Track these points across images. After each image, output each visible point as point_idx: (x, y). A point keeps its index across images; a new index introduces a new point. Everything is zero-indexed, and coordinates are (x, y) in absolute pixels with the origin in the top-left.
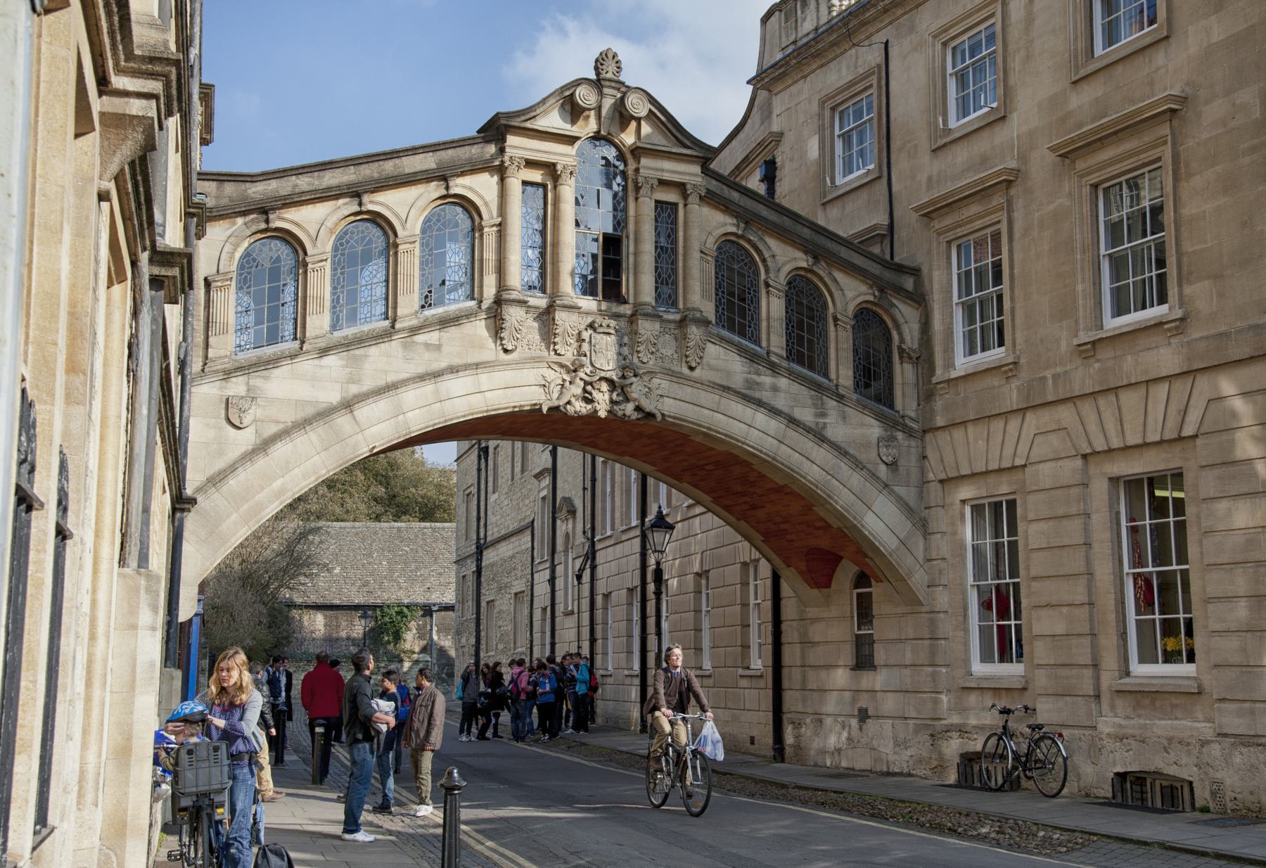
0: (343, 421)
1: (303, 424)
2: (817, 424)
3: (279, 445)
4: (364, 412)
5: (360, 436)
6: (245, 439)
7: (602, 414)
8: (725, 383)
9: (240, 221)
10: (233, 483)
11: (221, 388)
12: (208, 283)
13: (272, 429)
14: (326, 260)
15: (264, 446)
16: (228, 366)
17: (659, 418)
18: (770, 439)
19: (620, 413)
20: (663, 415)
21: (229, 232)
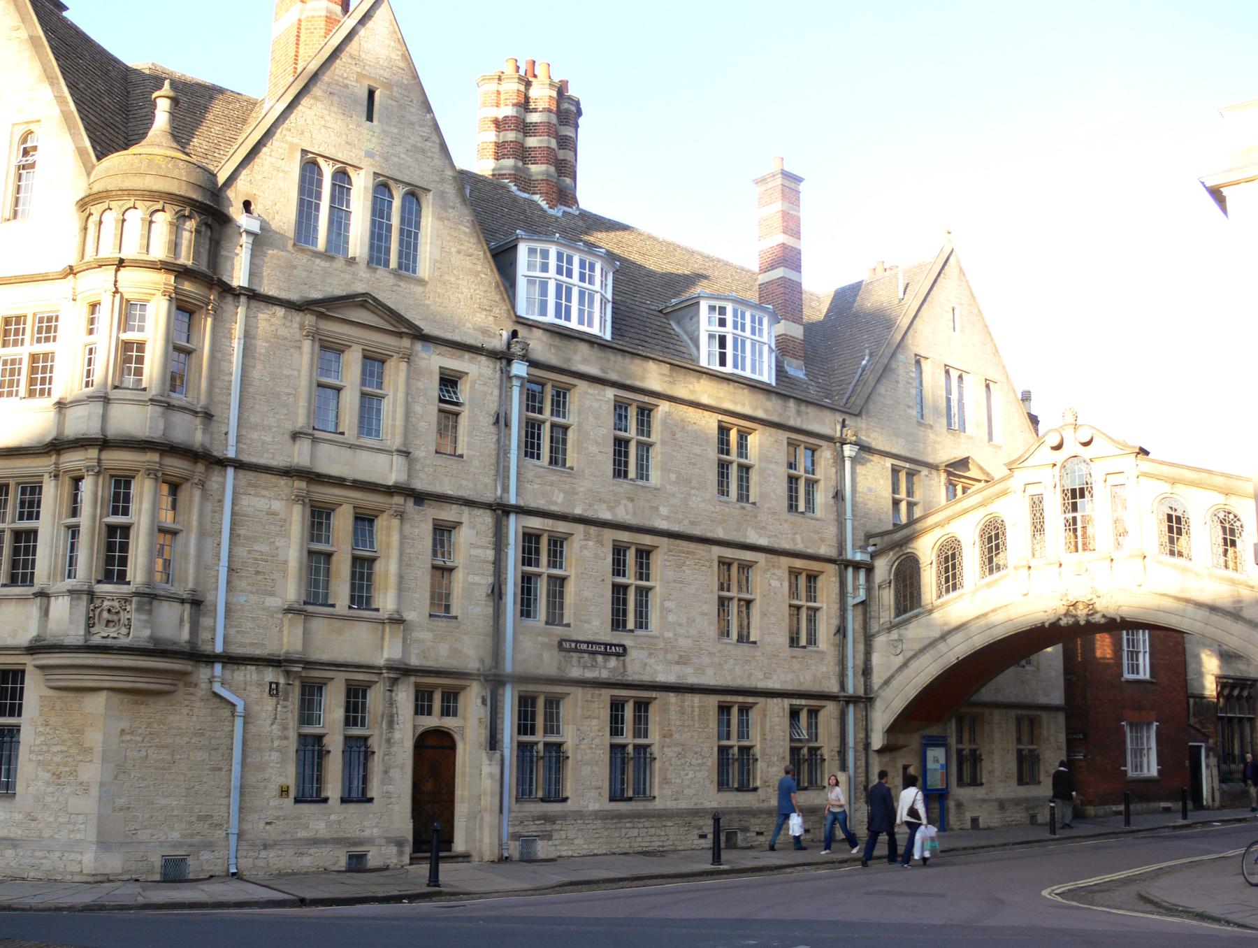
0: (942, 647)
1: (922, 651)
2: (1235, 608)
3: (912, 662)
4: (952, 640)
5: (950, 653)
6: (899, 661)
7: (1082, 623)
8: (1164, 592)
9: (891, 553)
10: (894, 683)
11: (888, 637)
12: (879, 587)
13: (911, 653)
14: (931, 564)
15: (905, 665)
16: (889, 626)
17: (1119, 620)
18: (1199, 623)
19: (1093, 621)
20: (1122, 618)
21: (887, 560)
